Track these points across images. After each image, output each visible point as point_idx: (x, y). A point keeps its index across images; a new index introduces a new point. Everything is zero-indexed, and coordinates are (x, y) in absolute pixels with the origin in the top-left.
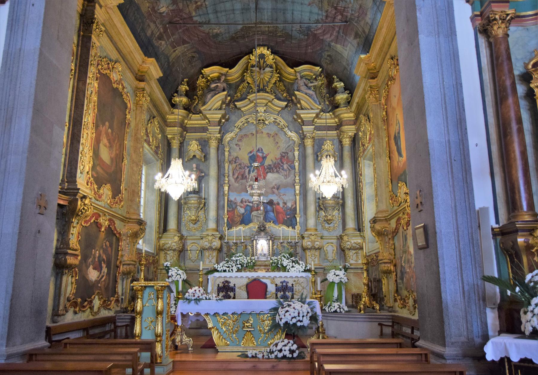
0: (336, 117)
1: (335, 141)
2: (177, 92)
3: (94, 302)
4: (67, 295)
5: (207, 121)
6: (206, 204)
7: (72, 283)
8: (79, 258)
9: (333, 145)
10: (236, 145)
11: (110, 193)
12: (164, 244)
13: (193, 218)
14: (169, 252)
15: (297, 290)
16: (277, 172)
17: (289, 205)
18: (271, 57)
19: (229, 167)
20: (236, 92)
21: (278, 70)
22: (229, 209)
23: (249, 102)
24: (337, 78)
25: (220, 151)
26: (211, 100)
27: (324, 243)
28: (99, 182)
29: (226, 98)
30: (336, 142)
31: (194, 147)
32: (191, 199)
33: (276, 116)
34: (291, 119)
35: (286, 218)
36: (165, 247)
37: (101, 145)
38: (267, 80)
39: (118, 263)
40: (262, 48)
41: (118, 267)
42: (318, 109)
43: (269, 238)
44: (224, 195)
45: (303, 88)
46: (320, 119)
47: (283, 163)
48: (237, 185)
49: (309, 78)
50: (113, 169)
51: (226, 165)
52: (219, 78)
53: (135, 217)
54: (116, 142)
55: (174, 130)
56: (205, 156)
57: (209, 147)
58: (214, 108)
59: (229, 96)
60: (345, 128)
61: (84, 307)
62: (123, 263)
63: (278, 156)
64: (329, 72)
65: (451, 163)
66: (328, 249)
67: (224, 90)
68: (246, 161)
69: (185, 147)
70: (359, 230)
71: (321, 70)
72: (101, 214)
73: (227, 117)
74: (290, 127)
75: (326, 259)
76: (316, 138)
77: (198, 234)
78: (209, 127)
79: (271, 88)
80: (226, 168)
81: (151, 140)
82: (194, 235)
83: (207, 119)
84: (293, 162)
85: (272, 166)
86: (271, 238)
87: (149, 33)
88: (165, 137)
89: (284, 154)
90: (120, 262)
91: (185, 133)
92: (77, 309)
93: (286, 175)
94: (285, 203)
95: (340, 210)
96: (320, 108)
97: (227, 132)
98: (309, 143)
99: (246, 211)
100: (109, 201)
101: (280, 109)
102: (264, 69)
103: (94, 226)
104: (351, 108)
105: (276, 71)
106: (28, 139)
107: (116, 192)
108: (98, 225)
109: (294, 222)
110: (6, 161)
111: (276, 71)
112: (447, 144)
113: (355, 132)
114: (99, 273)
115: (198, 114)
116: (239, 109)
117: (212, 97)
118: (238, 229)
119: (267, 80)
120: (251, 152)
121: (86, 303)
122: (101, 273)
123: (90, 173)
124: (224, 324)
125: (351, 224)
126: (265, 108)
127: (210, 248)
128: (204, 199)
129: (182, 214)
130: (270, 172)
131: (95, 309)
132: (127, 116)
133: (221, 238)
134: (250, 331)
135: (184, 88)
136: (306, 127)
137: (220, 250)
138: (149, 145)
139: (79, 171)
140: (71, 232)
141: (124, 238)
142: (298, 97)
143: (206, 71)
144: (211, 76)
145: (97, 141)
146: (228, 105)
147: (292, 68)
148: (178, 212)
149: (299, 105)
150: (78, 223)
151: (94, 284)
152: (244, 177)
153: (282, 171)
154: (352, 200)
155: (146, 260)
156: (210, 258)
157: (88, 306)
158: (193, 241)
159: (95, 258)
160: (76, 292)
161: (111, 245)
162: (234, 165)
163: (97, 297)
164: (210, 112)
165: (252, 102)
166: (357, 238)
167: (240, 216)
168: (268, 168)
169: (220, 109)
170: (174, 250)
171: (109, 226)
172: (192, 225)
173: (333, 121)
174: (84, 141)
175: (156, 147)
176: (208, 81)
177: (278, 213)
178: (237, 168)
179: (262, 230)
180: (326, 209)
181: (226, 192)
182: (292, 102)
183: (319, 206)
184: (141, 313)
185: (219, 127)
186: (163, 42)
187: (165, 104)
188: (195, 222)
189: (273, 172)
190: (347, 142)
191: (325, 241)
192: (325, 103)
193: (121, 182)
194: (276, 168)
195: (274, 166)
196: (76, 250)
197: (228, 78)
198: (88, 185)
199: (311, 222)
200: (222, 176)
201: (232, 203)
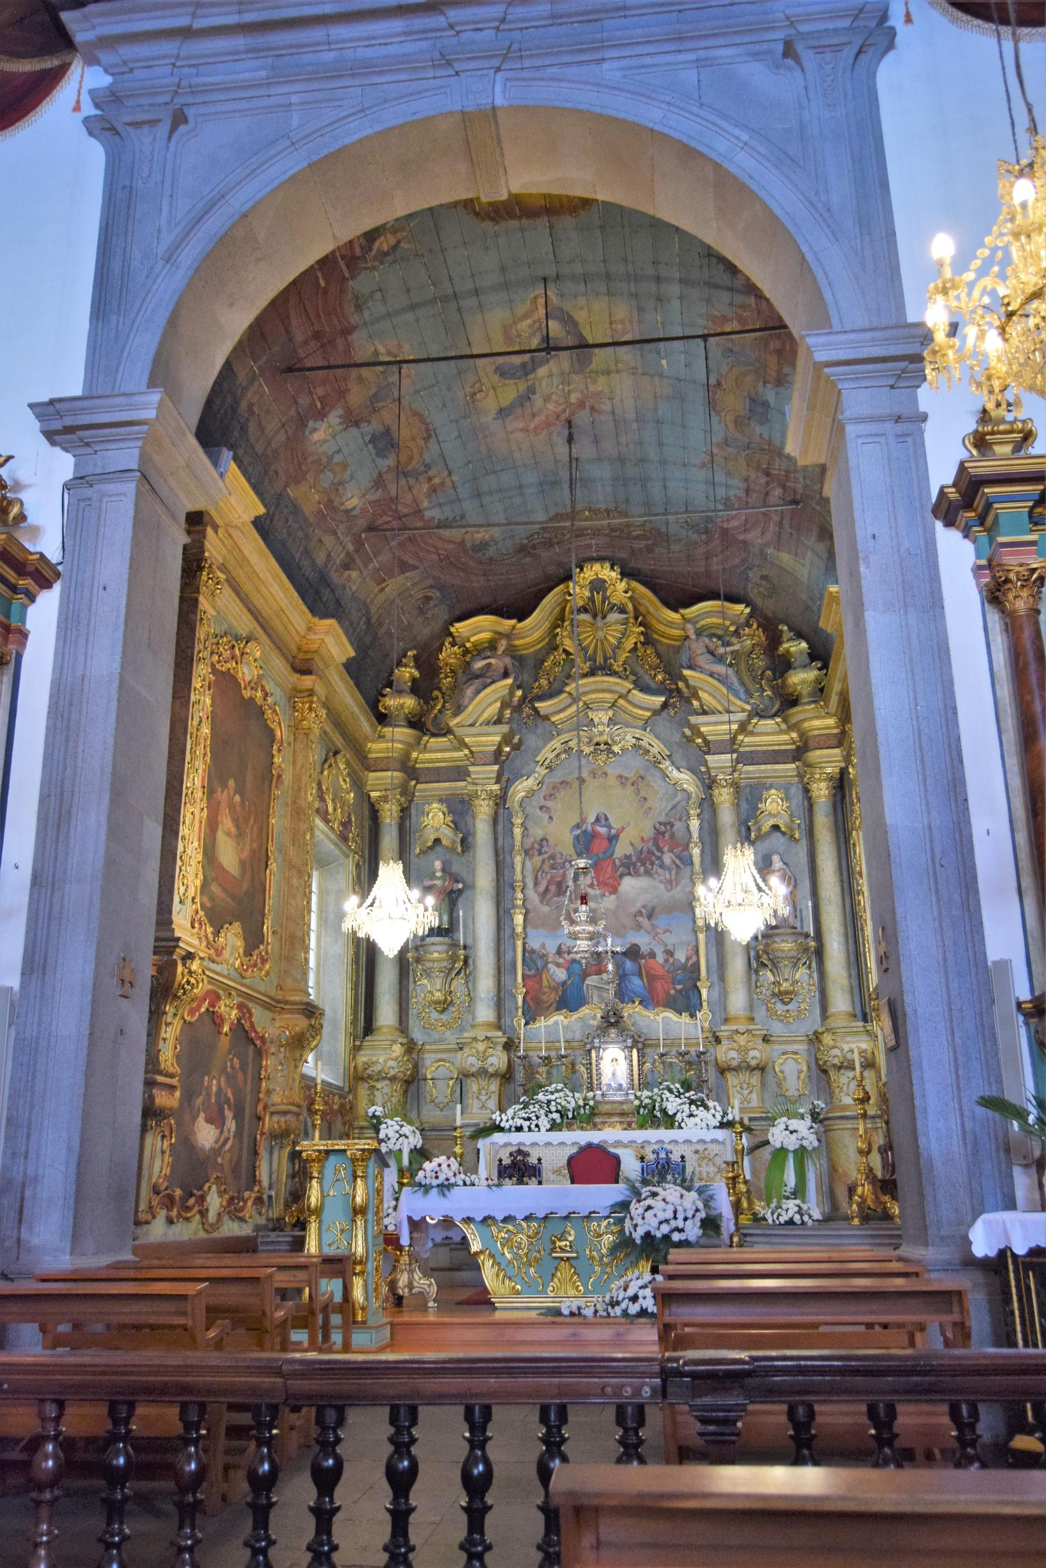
0: (791, 728)
1: (793, 790)
2: (390, 684)
3: (208, 1199)
4: (154, 1180)
5: (467, 752)
6: (470, 961)
7: (163, 1152)
8: (178, 1094)
9: (787, 798)
10: (541, 808)
11: (240, 943)
12: (367, 1065)
13: (438, 995)
14: (379, 1085)
15: (704, 1175)
16: (648, 873)
17: (681, 956)
18: (622, 586)
19: (524, 863)
20: (535, 679)
21: (640, 616)
22: (527, 972)
23: (570, 701)
24: (790, 629)
25: (500, 828)
26: (475, 702)
27: (775, 1054)
28: (216, 918)
29: (512, 693)
30: (796, 791)
31: (435, 820)
32: (432, 948)
33: (638, 733)
34: (677, 737)
35: (672, 992)
36: (369, 1072)
37: (220, 835)
38: (614, 641)
39: (260, 1108)
40: (597, 567)
41: (259, 1118)
42: (743, 711)
43: (629, 1042)
44: (513, 935)
45: (703, 660)
46: (752, 733)
47: (660, 850)
48: (546, 909)
49: (720, 632)
50: (245, 887)
51: (518, 860)
52: (492, 646)
53: (297, 998)
54: (251, 822)
55: (385, 778)
56: (463, 841)
57: (474, 818)
58: (481, 720)
59: (519, 687)
60: (815, 755)
61: (188, 1209)
62: (272, 1109)
63: (649, 833)
64: (770, 614)
65: (934, 869)
66: (784, 1068)
67: (506, 675)
69: (414, 819)
70: (865, 1019)
71: (748, 610)
72: (221, 992)
73: (516, 740)
74: (677, 757)
76: (743, 783)
77: (451, 1037)
78: (471, 769)
79: (624, 663)
80: (518, 868)
81: (330, 809)
82: (441, 1041)
83: (467, 746)
84: (686, 847)
85: (634, 859)
86: (635, 1043)
87: (320, 558)
88: (363, 796)
89: (663, 828)
90: (265, 1107)
91: (413, 783)
92: (174, 1213)
93: (670, 882)
94: (669, 953)
95: (814, 965)
96: (748, 707)
97: (518, 776)
98: (724, 796)
99: (570, 974)
100: (238, 963)
101: (649, 714)
102: (604, 617)
103: (207, 1020)
104: (827, 705)
105: (636, 618)
106: (102, 851)
107: (254, 940)
108: (215, 1019)
109: (694, 1000)
110: (63, 896)
111: (636, 618)
112: (927, 832)
113: (843, 765)
114: (217, 1132)
115: (444, 735)
116: (546, 718)
118: (551, 1021)
119: (614, 641)
120: (578, 826)
121: (192, 1201)
122: (222, 1132)
123: (198, 900)
124: (506, 1242)
125: (841, 1002)
126: (610, 713)
127: (482, 1073)
128: (465, 947)
129: (411, 986)
130: (629, 874)
131: (212, 1216)
132: (276, 760)
133: (509, 1046)
134: (568, 1259)
135: (407, 673)
136: (716, 757)
137: (507, 1077)
138: (327, 821)
139: (176, 899)
140: (163, 1035)
141: (273, 1050)
142: (691, 682)
143: (460, 628)
144: (472, 639)
145: (212, 825)
146: (518, 709)
147: (676, 611)
148: (400, 983)
149: (695, 703)
150: (175, 1015)
151: (208, 1157)
153: (660, 871)
154: (842, 939)
155: (326, 1103)
156: (483, 1098)
157: (196, 1209)
158: (439, 1056)
159: (209, 1095)
160: (172, 1171)
161: (243, 1068)
162: (537, 860)
163: (214, 1188)
164: (472, 730)
165: (575, 700)
166: (857, 1038)
167: (556, 989)
168: (623, 865)
169: (499, 721)
170: (393, 1079)
171: (239, 1020)
172: (435, 1015)
173: (785, 737)
174: (186, 831)
175: (343, 824)
176: (467, 651)
177: (652, 978)
178: (546, 868)
179: (612, 1025)
180: (775, 966)
181: (519, 929)
182: (677, 697)
183: (758, 957)
184: (318, 1212)
185: (496, 767)
186: (354, 574)
187: (362, 719)
188: (444, 1006)
189: (637, 874)
190: (821, 791)
191: (776, 1047)
192: (761, 696)
193: (263, 915)
194: (644, 864)
195: (639, 859)
196: (172, 1076)
197: (517, 643)
198: (193, 927)
199: (738, 1001)
200: (507, 889)
201: (534, 956)
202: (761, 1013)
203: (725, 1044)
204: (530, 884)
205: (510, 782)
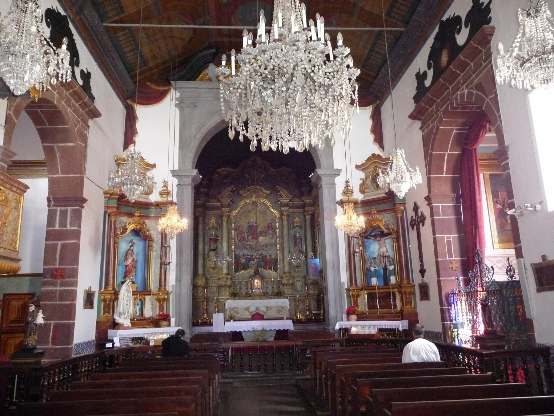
0: (303, 201)
13: (213, 266)
17: (273, 257)
30: (302, 217)
44: (232, 251)
51: (233, 231)
63: (266, 225)
68: (246, 229)
75: (296, 290)
80: (233, 234)
84: (275, 230)
116: (241, 195)
117: (225, 189)
127: (225, 286)
137: (230, 286)
152: (244, 239)
172: (212, 271)
202: (292, 271)
203: (284, 279)
204: (236, 237)
205: (231, 211)
